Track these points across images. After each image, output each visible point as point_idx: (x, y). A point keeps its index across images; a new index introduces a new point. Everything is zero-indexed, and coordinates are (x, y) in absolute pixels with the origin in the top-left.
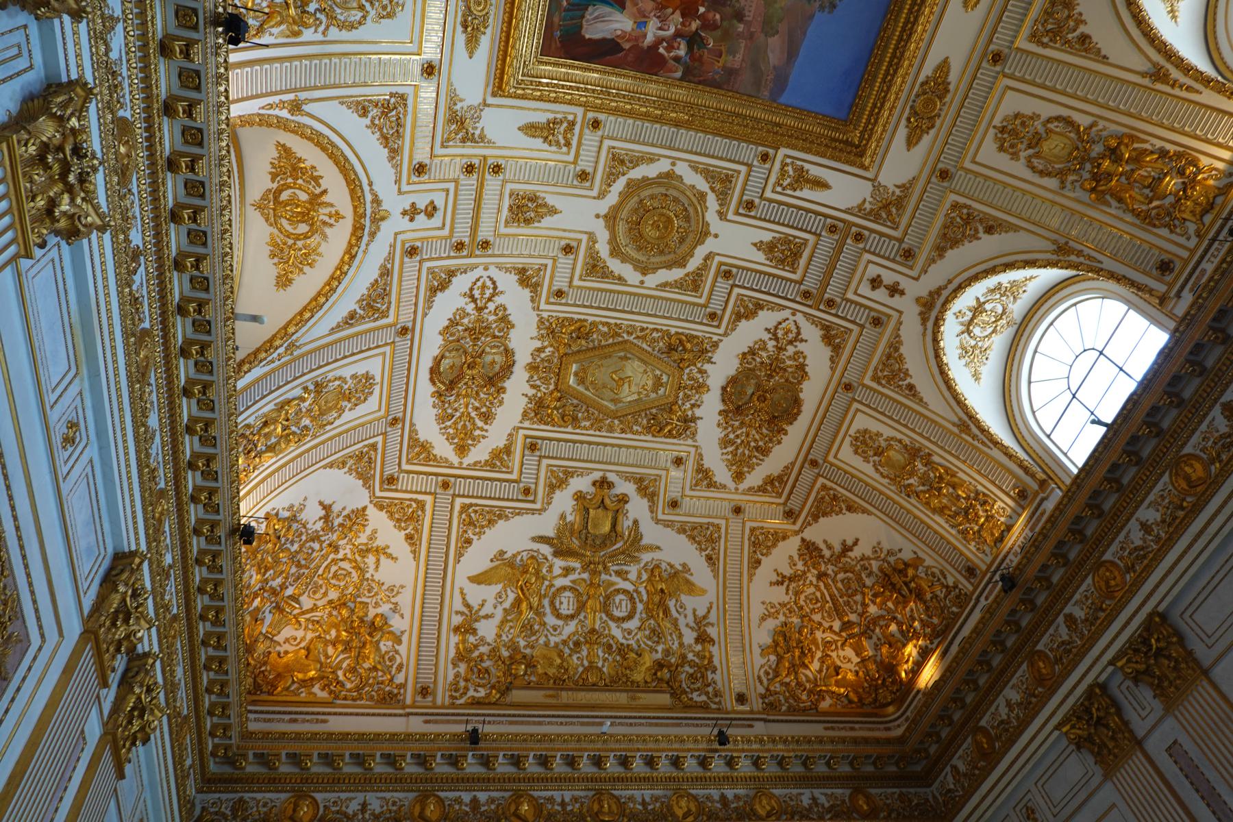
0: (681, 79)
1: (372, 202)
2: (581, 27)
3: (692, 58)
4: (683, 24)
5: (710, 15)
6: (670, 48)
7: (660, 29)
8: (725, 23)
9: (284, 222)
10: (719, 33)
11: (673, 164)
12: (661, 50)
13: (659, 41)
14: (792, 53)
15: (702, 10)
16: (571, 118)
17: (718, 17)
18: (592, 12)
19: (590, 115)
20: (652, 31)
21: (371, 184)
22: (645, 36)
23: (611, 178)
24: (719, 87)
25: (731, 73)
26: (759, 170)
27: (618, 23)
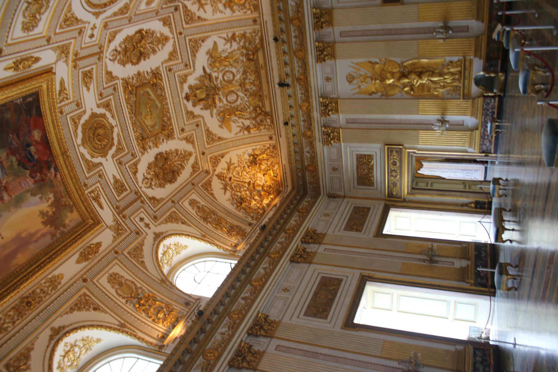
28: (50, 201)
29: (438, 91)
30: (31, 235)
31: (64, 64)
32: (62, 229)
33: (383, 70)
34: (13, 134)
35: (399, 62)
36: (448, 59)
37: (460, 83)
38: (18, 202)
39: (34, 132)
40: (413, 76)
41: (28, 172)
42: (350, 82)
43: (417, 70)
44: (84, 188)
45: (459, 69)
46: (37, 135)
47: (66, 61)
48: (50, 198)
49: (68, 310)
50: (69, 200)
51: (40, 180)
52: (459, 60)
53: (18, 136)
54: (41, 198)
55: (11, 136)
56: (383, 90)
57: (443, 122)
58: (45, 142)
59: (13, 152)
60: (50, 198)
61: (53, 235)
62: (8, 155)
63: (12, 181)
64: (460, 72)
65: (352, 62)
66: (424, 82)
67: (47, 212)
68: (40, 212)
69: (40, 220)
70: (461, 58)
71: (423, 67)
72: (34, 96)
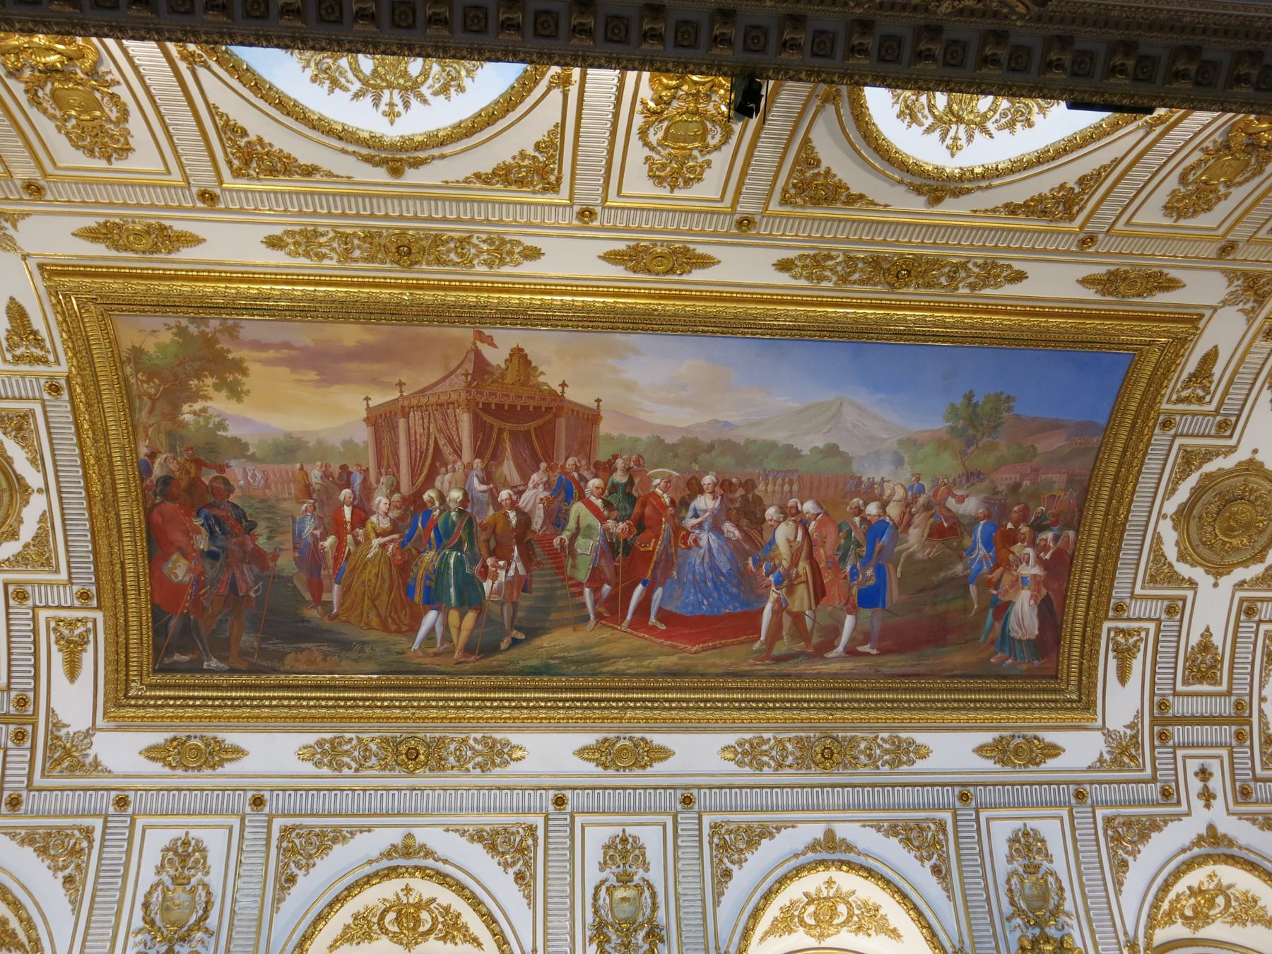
0: (1077, 531)
1: (1200, 846)
2: (1029, 640)
3: (1055, 523)
4: (1023, 541)
5: (1015, 516)
6: (1045, 548)
7: (1028, 563)
8: (1022, 499)
9: (1212, 913)
10: (1031, 504)
11: (1165, 516)
12: (1047, 557)
13: (1039, 561)
14: (1053, 426)
15: (1010, 526)
16: (1112, 634)
17: (1016, 509)
18: (1015, 631)
19: (1111, 614)
20: (1031, 570)
21: (1184, 851)
22: (1035, 576)
23: (1174, 579)
24: (1086, 491)
25: (1071, 481)
26: (1184, 424)
27: (1024, 608)
28: (197, 406)
30: (293, 364)
31: (63, 715)
32: (193, 329)
34: (250, 597)
38: (288, 449)
39: (187, 579)
41: (232, 499)
44: (63, 382)
46: (179, 570)
47: (55, 725)
48: (195, 413)
49: (318, 177)
50: (133, 381)
51: (206, 465)
53: (233, 586)
54: (222, 425)
55: (252, 594)
58: (157, 544)
59: (258, 557)
60: (195, 413)
61: (232, 332)
62: (275, 557)
63: (285, 500)
67: (217, 388)
68: (239, 400)
69: (248, 383)
72: (167, 661)
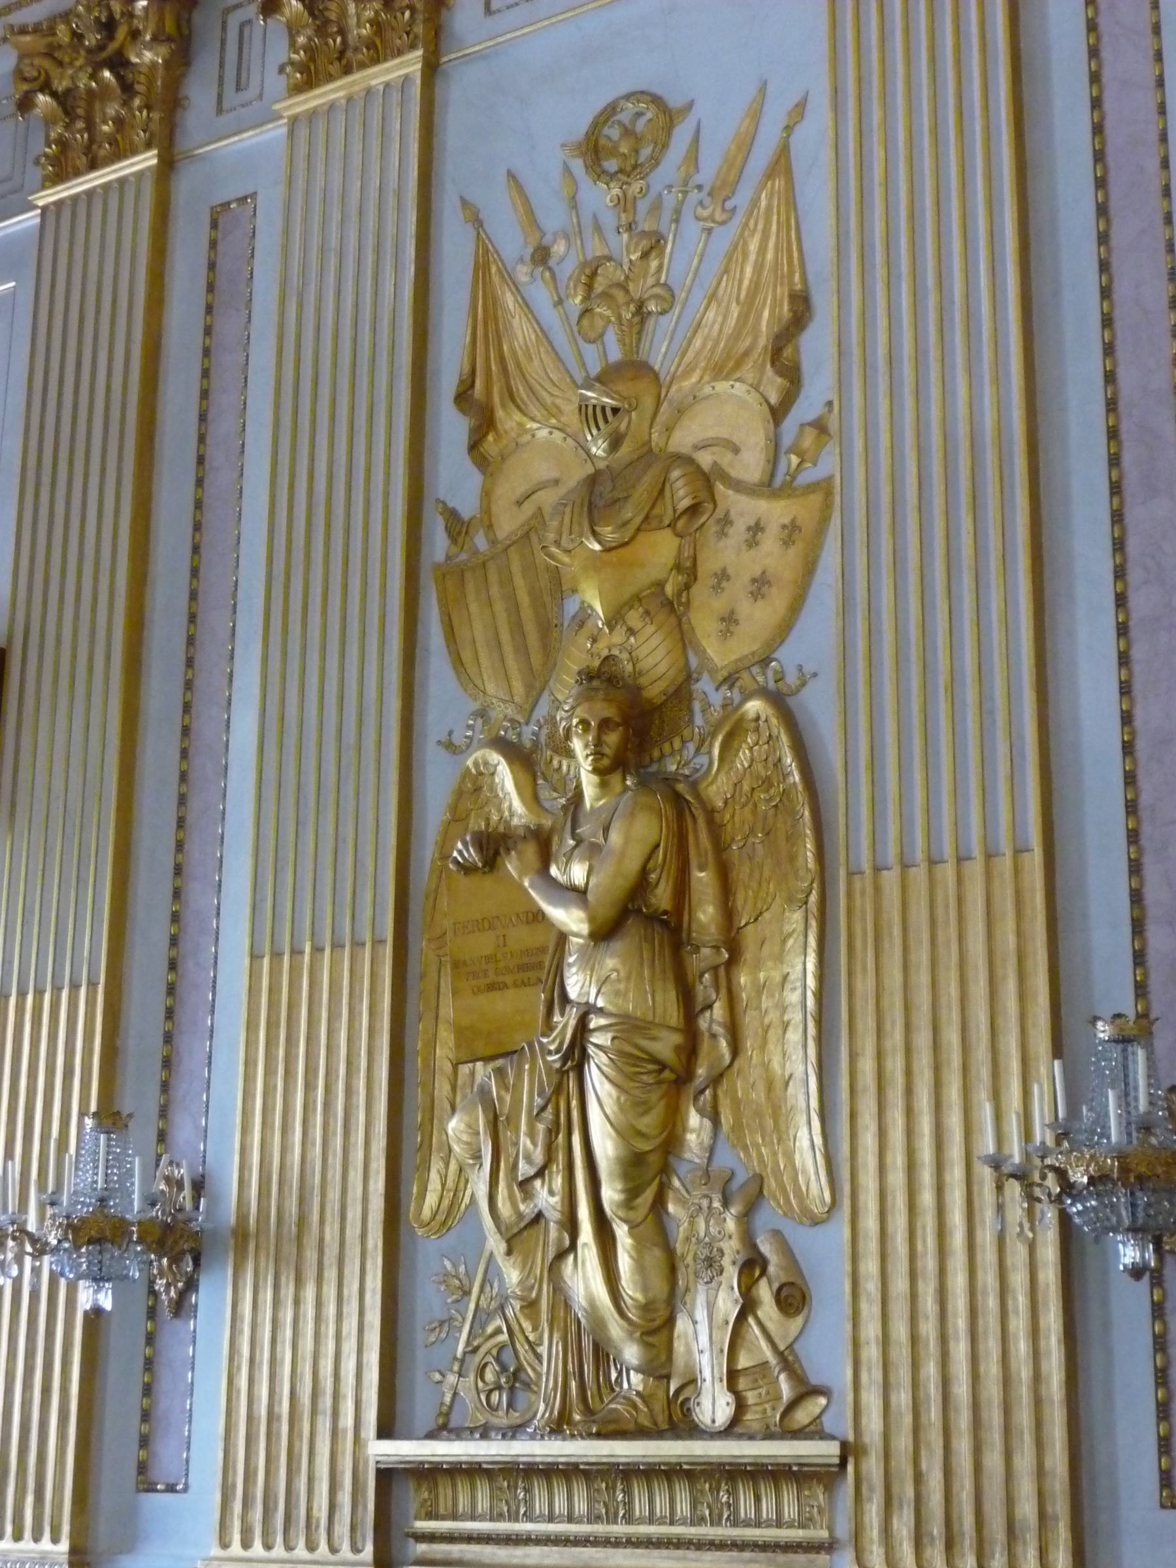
29: (477, 1156)
33: (706, 482)
35: (788, 656)
36: (824, 1253)
37: (558, 1427)
40: (633, 835)
42: (593, 149)
43: (703, 878)
45: (714, 1406)
52: (806, 1391)
56: (508, 523)
57: (167, 1244)
64: (679, 1421)
65: (800, 109)
66: (576, 984)
70: (840, 1422)
71: (732, 945)
